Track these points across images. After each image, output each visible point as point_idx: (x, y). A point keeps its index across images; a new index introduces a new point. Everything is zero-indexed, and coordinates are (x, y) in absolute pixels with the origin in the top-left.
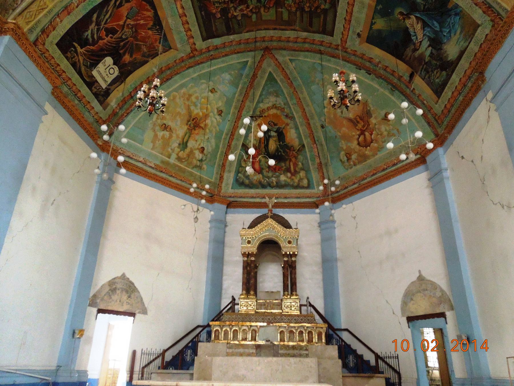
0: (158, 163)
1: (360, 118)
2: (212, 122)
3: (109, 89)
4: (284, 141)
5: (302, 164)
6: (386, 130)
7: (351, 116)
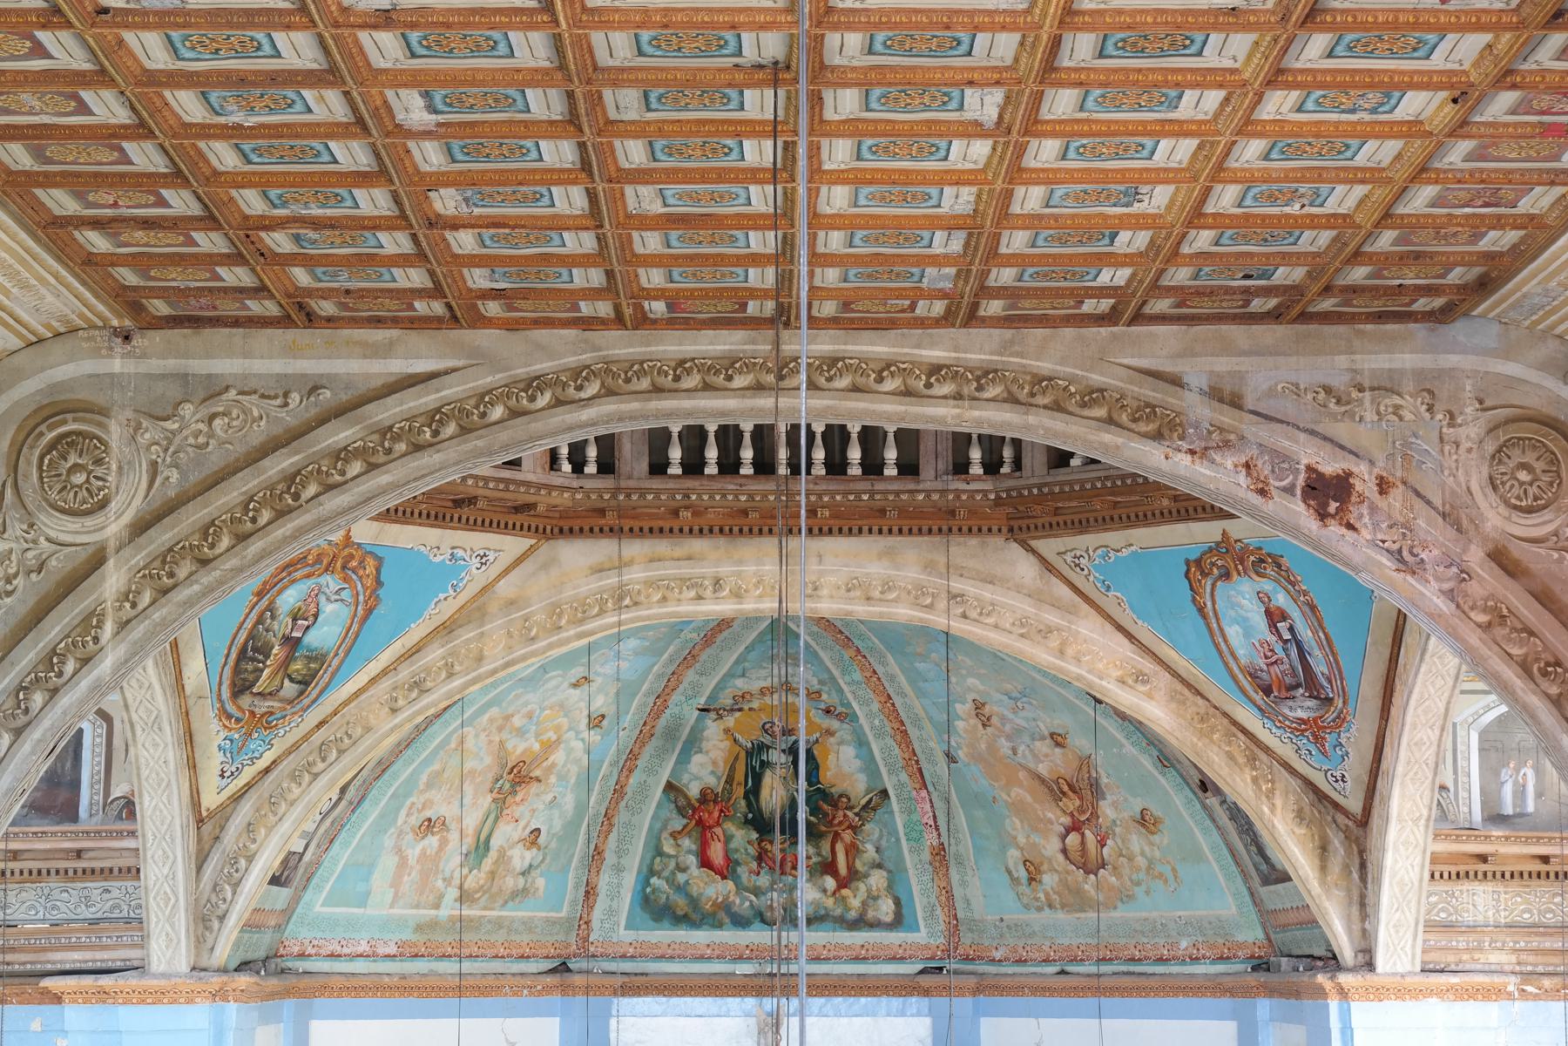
0: (408, 935)
5: (878, 850)
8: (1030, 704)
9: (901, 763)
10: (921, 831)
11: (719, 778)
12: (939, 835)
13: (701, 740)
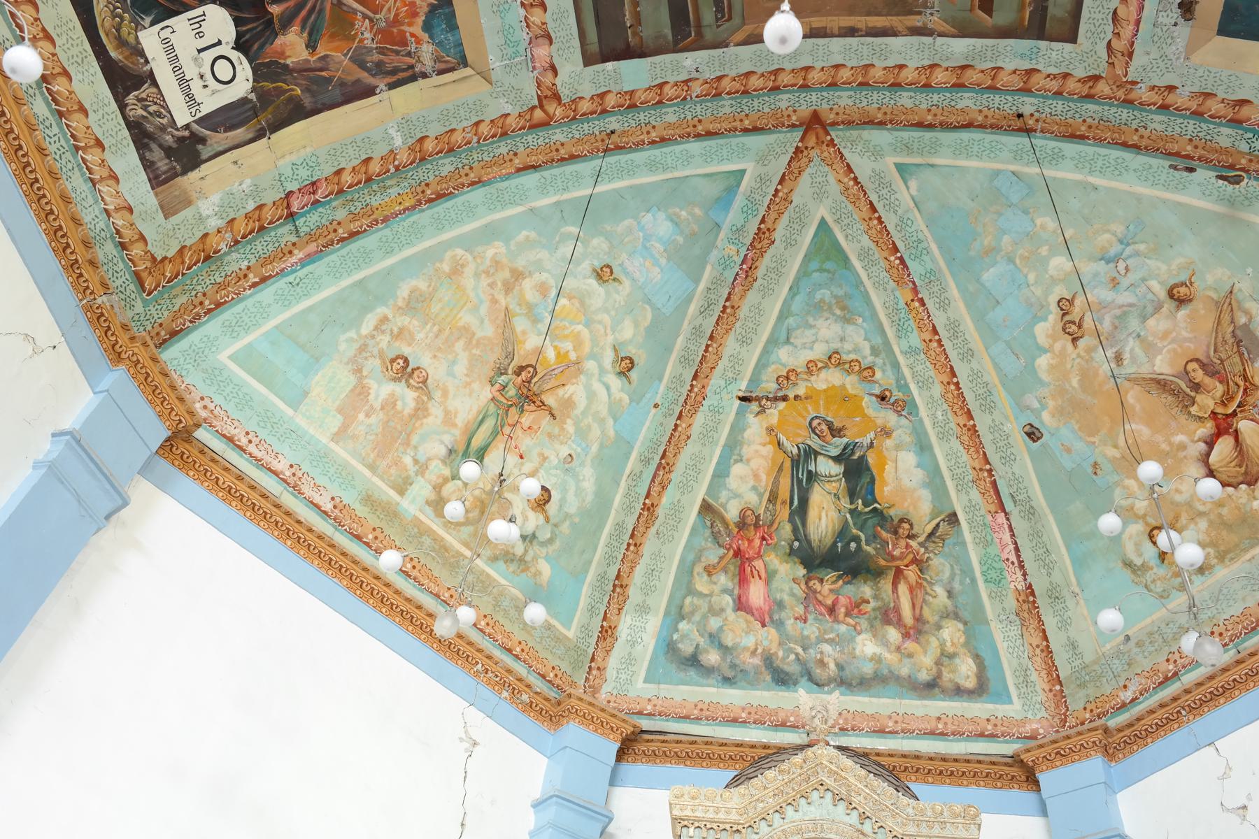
0: (350, 498)
1: (1203, 366)
2: (591, 396)
3: (203, 140)
4: (870, 498)
5: (950, 594)
7: (1163, 365)
8: (1137, 254)
9: (971, 475)
10: (1002, 570)
11: (761, 496)
12: (1025, 575)
13: (742, 444)
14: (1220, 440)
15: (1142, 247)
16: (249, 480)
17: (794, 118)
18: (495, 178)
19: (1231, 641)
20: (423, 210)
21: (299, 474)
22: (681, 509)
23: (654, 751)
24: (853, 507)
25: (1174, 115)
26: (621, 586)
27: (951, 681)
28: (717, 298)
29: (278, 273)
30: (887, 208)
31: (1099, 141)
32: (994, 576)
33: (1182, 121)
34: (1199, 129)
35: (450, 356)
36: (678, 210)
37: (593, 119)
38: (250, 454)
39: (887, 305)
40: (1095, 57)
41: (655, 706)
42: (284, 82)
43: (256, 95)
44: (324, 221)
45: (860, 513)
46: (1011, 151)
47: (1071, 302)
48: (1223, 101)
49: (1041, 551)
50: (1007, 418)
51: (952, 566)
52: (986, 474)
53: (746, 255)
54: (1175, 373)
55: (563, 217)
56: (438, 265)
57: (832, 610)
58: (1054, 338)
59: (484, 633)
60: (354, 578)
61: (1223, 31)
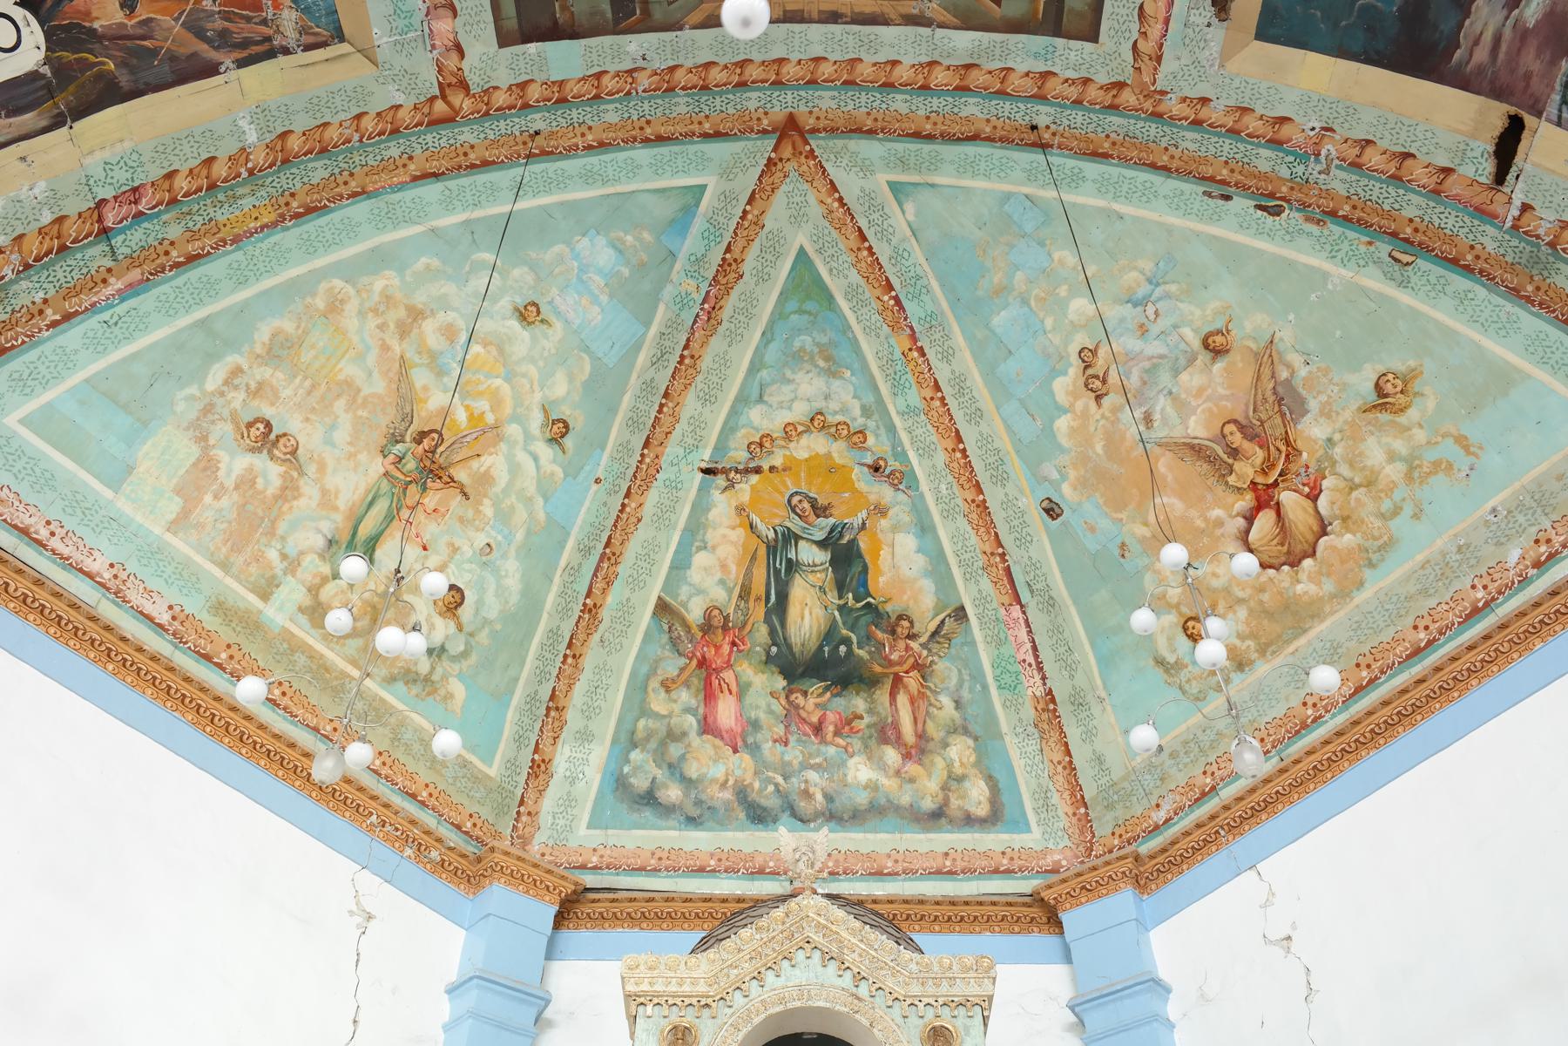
0: (193, 605)
1: (1242, 428)
2: (515, 469)
4: (863, 591)
5: (958, 704)
6: (1392, 457)
7: (1197, 428)
8: (1167, 296)
9: (981, 561)
10: (1017, 674)
11: (730, 591)
12: (1044, 678)
13: (705, 527)
14: (1261, 514)
15: (1173, 288)
16: (52, 585)
17: (765, 122)
18: (383, 187)
19: (1274, 747)
20: (288, 229)
21: (123, 576)
22: (631, 610)
23: (601, 914)
24: (842, 602)
25: (1208, 132)
26: (557, 709)
27: (960, 808)
28: (672, 345)
29: (87, 309)
30: (879, 235)
31: (1125, 160)
32: (1009, 681)
33: (1216, 139)
34: (1235, 150)
35: (326, 419)
36: (622, 234)
37: (512, 116)
38: (53, 551)
39: (880, 355)
40: (1119, 60)
41: (602, 856)
42: (91, 52)
43: (51, 68)
44: (150, 240)
45: (851, 610)
46: (1024, 170)
47: (1094, 352)
48: (1261, 118)
49: (1062, 650)
50: (1021, 491)
51: (959, 671)
52: (998, 559)
53: (708, 293)
54: (1210, 437)
55: (474, 241)
56: (309, 300)
57: (818, 729)
58: (1075, 396)
59: (380, 775)
60: (202, 710)
61: (1262, 35)
